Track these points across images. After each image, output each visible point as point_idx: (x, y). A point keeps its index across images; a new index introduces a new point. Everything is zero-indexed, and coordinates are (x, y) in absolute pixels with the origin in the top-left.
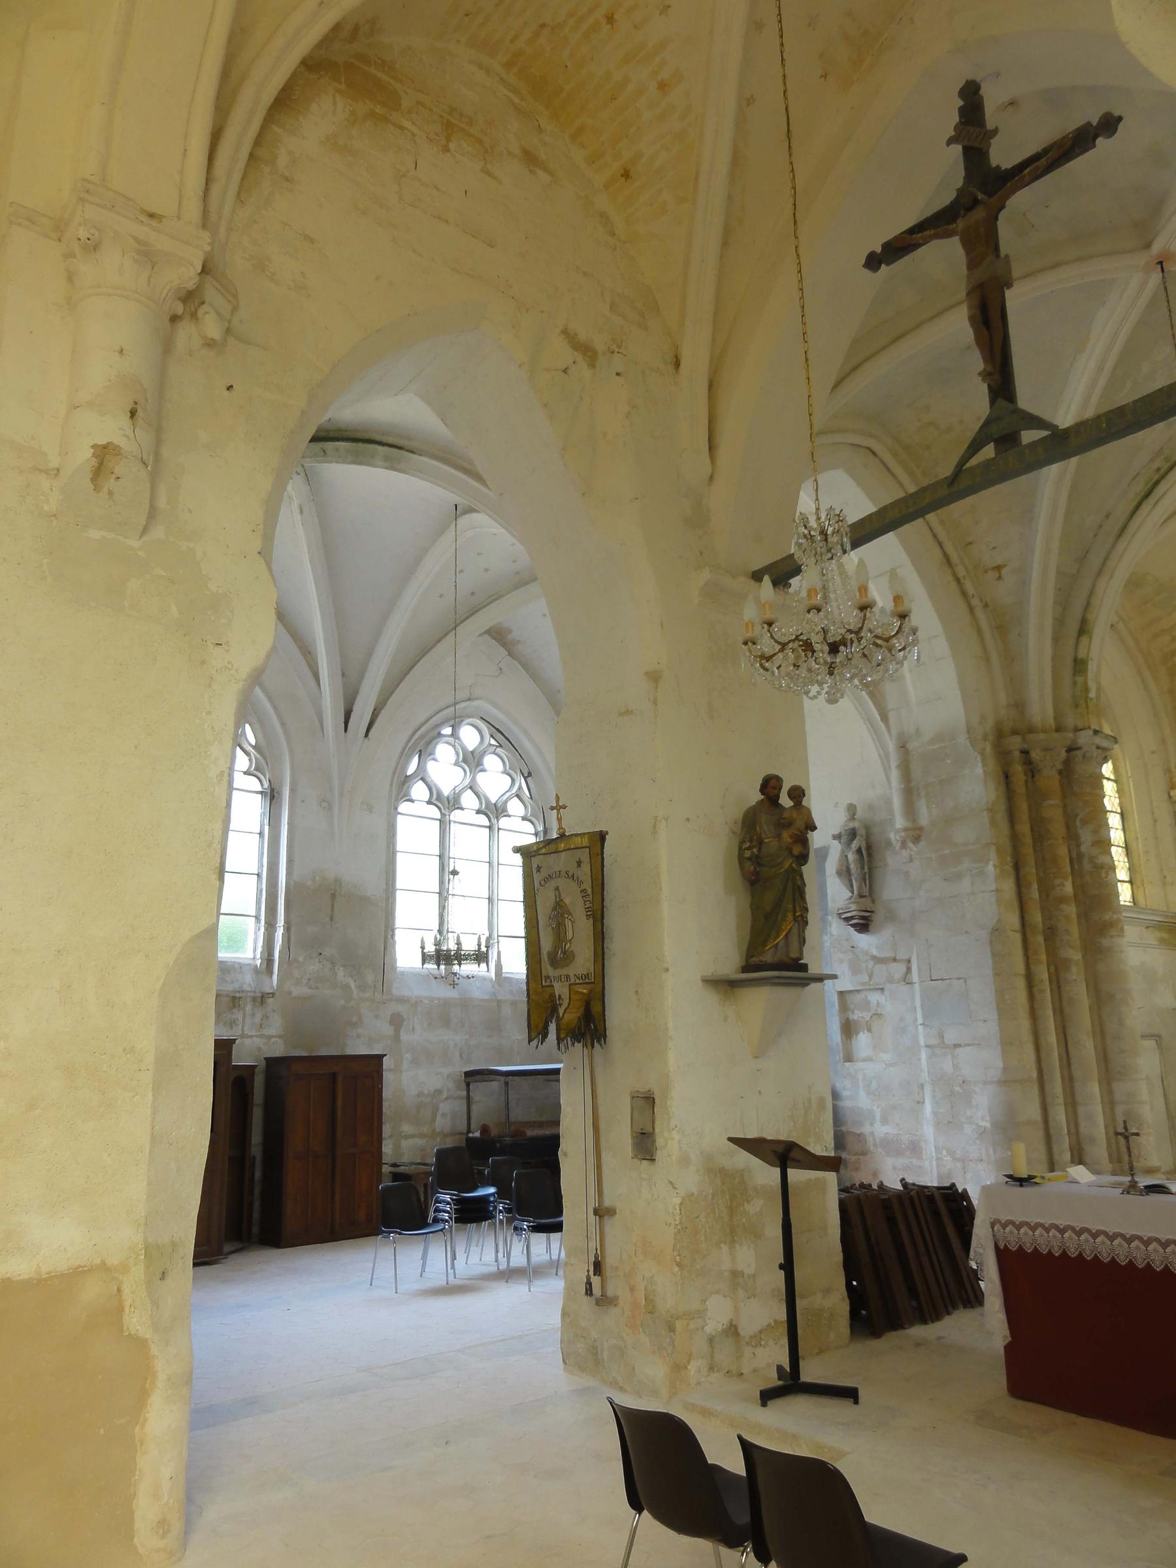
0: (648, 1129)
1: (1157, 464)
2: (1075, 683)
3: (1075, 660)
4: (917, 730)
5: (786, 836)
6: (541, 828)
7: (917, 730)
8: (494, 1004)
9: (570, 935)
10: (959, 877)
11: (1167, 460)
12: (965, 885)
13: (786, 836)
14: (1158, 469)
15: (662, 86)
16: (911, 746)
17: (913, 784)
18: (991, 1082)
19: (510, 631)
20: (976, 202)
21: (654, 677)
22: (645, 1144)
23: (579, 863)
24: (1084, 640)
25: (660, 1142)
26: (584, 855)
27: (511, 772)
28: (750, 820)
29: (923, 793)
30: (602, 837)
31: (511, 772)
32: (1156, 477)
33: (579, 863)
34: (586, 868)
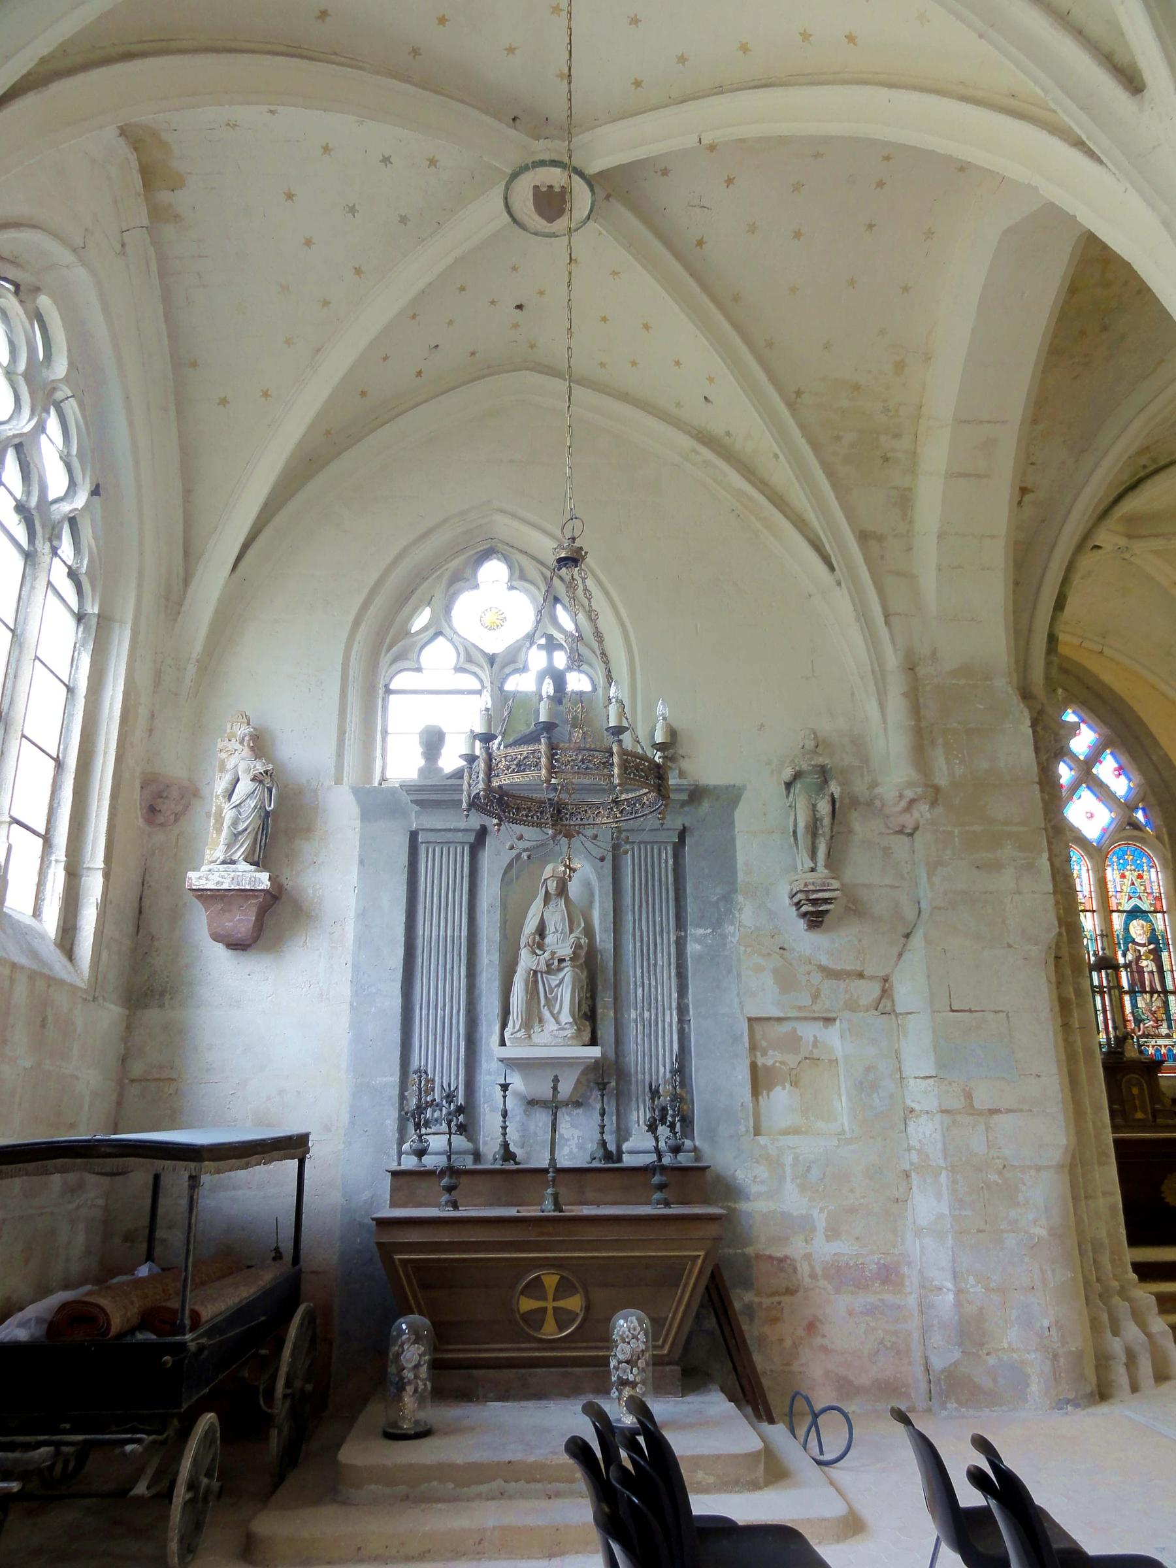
1: (1143, 460)
4: (934, 653)
6: (93, 609)
7: (934, 653)
8: (7, 971)
10: (996, 866)
11: (1154, 460)
12: (1006, 879)
14: (1145, 467)
16: (922, 671)
17: (923, 724)
18: (1048, 1167)
19: (176, 183)
27: (76, 464)
29: (940, 741)
31: (76, 464)
32: (1142, 474)
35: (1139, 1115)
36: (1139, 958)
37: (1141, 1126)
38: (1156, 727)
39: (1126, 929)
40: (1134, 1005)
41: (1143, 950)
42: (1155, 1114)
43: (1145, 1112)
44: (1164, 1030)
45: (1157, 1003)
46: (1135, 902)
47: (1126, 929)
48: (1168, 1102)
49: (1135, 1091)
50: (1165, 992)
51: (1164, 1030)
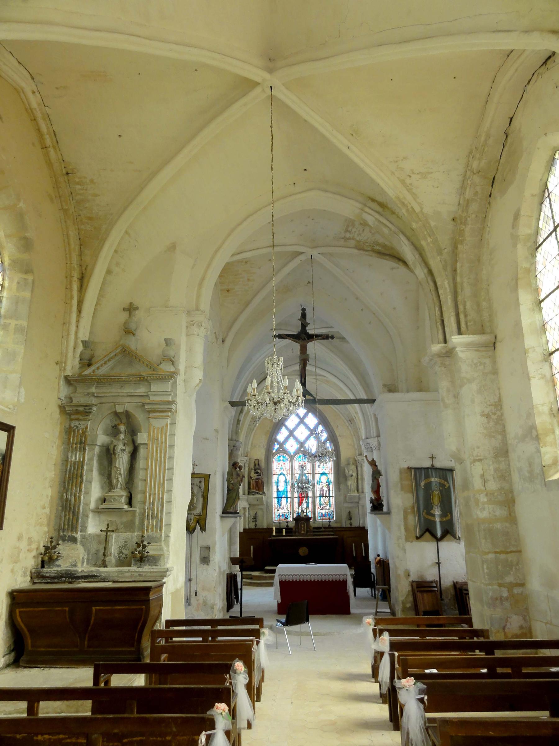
0: (207, 555)
2: (237, 427)
3: (238, 420)
5: (239, 479)
9: (195, 502)
13: (239, 479)
15: (248, 280)
20: (305, 339)
21: (217, 431)
22: (205, 560)
23: (200, 482)
24: (241, 414)
25: (211, 559)
26: (203, 480)
28: (230, 474)
30: (209, 475)
33: (200, 482)
34: (203, 483)
35: (303, 532)
36: (323, 487)
37: (303, 535)
38: (330, 420)
39: (320, 479)
40: (320, 501)
41: (324, 485)
42: (307, 532)
43: (304, 531)
44: (328, 507)
45: (327, 499)
46: (324, 470)
47: (320, 479)
48: (311, 528)
49: (303, 526)
50: (330, 497)
51: (328, 507)
